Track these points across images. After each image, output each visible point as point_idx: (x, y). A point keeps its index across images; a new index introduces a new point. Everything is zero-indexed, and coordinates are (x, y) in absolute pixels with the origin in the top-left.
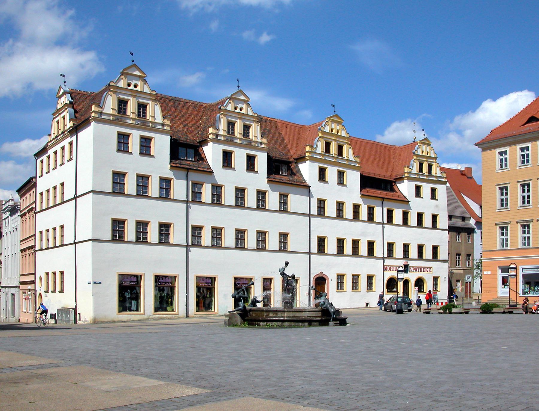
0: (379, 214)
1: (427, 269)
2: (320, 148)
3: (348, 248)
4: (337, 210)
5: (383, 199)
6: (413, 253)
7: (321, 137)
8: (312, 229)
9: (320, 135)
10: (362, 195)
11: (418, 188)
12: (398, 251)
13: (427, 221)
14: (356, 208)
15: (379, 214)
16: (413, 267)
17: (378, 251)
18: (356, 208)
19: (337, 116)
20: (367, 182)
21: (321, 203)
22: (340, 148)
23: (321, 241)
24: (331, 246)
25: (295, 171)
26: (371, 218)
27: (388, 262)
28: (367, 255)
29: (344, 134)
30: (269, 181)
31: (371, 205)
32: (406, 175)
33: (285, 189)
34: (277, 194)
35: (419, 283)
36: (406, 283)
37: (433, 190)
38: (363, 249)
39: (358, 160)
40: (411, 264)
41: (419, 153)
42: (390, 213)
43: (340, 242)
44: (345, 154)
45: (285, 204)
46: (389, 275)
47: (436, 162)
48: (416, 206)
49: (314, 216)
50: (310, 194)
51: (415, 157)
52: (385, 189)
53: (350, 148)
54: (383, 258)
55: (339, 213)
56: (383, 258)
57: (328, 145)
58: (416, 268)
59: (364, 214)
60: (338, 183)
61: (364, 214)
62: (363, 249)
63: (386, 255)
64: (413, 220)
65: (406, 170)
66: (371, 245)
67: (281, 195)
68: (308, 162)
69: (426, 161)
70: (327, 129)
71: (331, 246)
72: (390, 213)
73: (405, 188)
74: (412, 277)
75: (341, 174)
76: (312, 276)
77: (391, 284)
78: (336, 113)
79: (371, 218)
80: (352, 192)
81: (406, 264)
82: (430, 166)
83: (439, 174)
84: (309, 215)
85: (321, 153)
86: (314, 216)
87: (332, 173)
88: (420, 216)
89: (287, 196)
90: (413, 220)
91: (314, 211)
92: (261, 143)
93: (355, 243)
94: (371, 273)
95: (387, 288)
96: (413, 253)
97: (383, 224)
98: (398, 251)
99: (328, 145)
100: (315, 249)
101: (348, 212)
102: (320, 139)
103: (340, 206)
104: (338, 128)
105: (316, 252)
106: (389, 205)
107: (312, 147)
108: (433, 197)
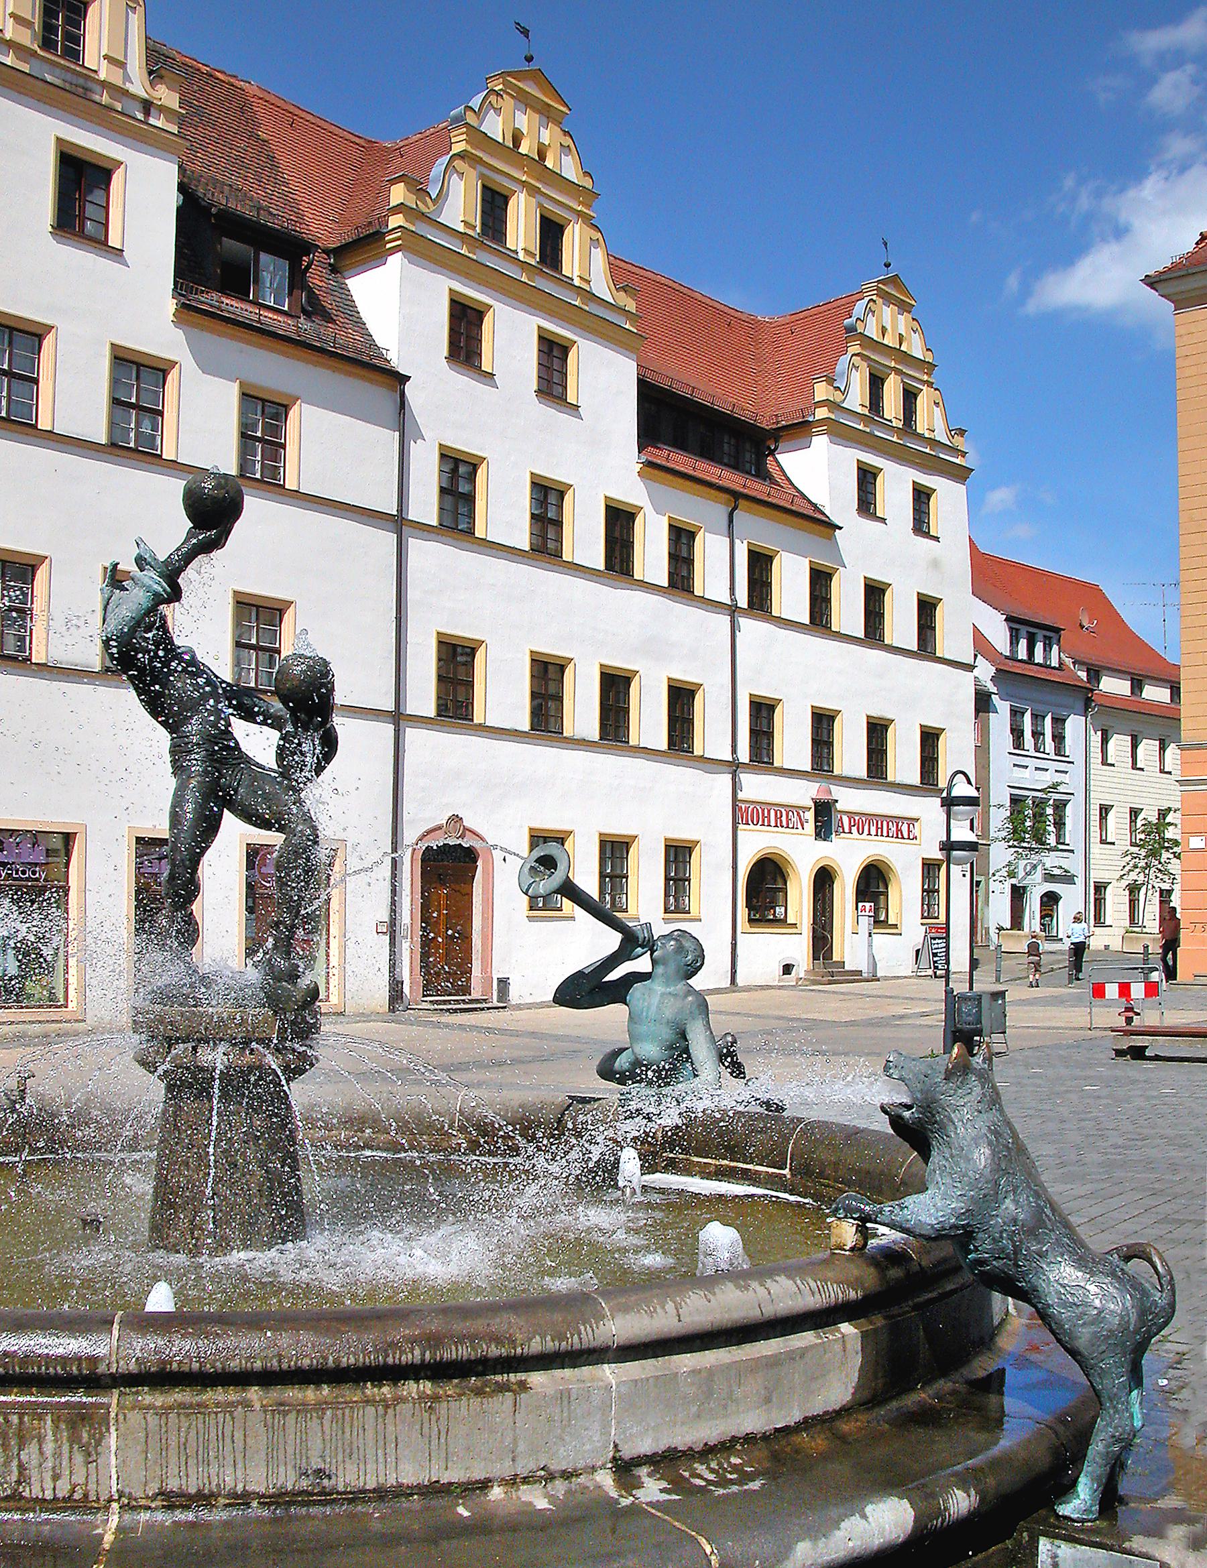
0: (718, 565)
1: (899, 827)
2: (459, 206)
3: (582, 709)
4: (533, 516)
5: (736, 496)
6: (851, 754)
7: (461, 156)
8: (412, 595)
9: (456, 149)
10: (650, 464)
11: (867, 477)
12: (793, 742)
14: (620, 521)
15: (718, 565)
16: (850, 814)
17: (715, 732)
18: (620, 521)
19: (538, 76)
20: (668, 420)
21: (459, 475)
22: (551, 232)
23: (457, 658)
24: (503, 694)
25: (328, 302)
26: (681, 579)
27: (756, 786)
28: (664, 746)
29: (570, 169)
30: (188, 312)
31: (685, 519)
32: (822, 413)
33: (275, 371)
34: (231, 393)
35: (873, 882)
36: (824, 879)
37: (922, 496)
38: (649, 720)
39: (631, 306)
40: (848, 800)
41: (872, 331)
42: (760, 563)
43: (547, 675)
44: (571, 265)
45: (275, 449)
46: (756, 842)
47: (930, 384)
48: (863, 549)
49: (423, 529)
50: (401, 419)
51: (855, 349)
52: (736, 465)
53: (594, 243)
54: (734, 767)
55: (544, 538)
56: (734, 767)
57: (494, 205)
58: (863, 821)
59: (651, 553)
60: (539, 392)
61: (651, 553)
62: (649, 720)
63: (744, 755)
64: (848, 611)
65: (822, 391)
66: (681, 698)
67: (247, 397)
68: (396, 260)
69: (898, 372)
70: (494, 126)
71: (503, 694)
72: (760, 563)
73: (816, 469)
74: (848, 855)
75: (553, 353)
76: (410, 835)
77: (764, 886)
78: (533, 66)
79: (681, 579)
80: (600, 450)
81: (824, 797)
82: (910, 397)
84: (399, 523)
85: (461, 228)
86: (423, 529)
87: (512, 335)
88: (875, 593)
89: (287, 408)
90: (848, 611)
91: (425, 505)
92: (147, 106)
93: (615, 687)
94: (682, 834)
95: (749, 905)
96: (851, 754)
97: (733, 610)
98: (793, 742)
99: (494, 205)
100: (423, 697)
101: (585, 538)
102: (458, 163)
103: (547, 498)
104: (546, 136)
105: (430, 710)
106: (757, 529)
107: (421, 192)
108: (921, 525)
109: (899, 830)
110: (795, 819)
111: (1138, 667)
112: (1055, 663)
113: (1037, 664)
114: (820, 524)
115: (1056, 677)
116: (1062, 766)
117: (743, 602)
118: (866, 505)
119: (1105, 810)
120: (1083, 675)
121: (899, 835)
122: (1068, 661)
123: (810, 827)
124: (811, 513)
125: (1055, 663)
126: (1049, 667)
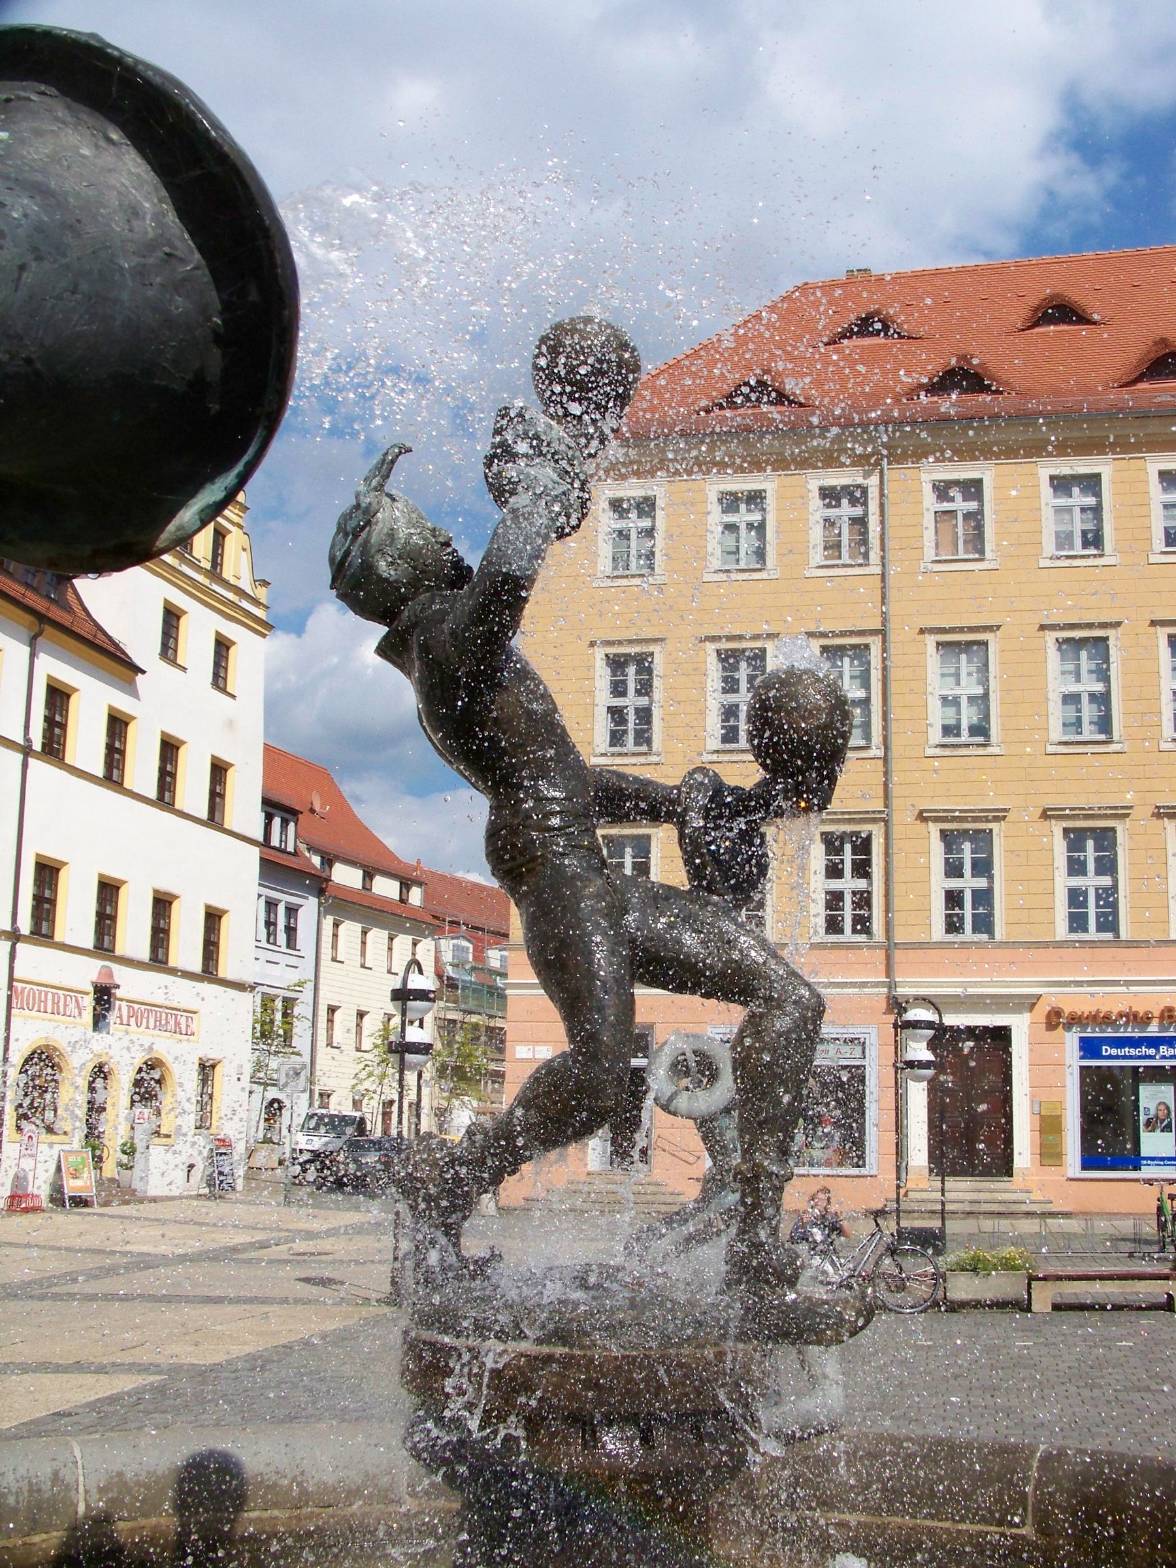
1: (176, 1020)
11: (172, 617)
12: (76, 915)
13: (192, 789)
27: (34, 961)
35: (148, 1086)
37: (222, 646)
40: (133, 984)
47: (240, 527)
58: (144, 1010)
63: (25, 925)
81: (105, 981)
83: (246, 584)
88: (169, 748)
97: (26, 751)
98: (76, 915)
108: (219, 679)
109: (177, 1024)
110: (72, 1005)
111: (372, 859)
112: (290, 849)
113: (274, 848)
114: (116, 662)
115: (293, 862)
116: (293, 961)
117: (37, 746)
118: (169, 649)
119: (332, 1010)
120: (316, 860)
121: (177, 1030)
122: (303, 847)
123: (88, 1016)
124: (112, 649)
125: (290, 849)
126: (284, 851)
